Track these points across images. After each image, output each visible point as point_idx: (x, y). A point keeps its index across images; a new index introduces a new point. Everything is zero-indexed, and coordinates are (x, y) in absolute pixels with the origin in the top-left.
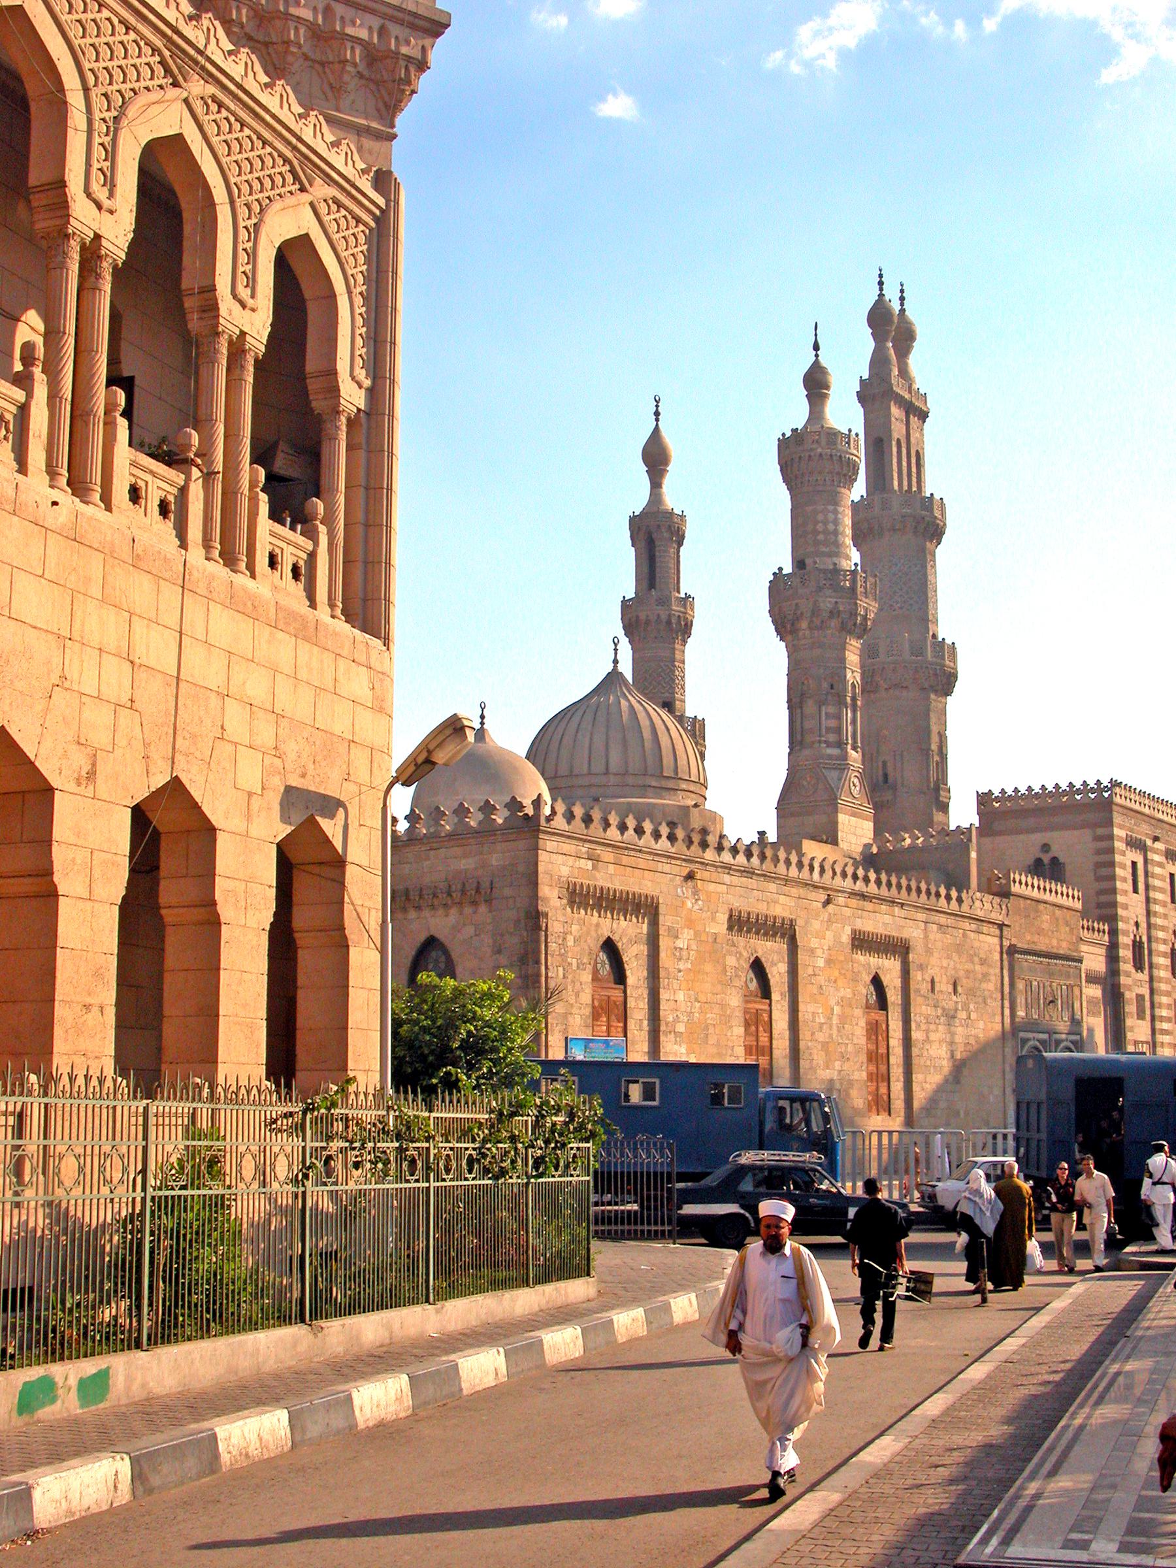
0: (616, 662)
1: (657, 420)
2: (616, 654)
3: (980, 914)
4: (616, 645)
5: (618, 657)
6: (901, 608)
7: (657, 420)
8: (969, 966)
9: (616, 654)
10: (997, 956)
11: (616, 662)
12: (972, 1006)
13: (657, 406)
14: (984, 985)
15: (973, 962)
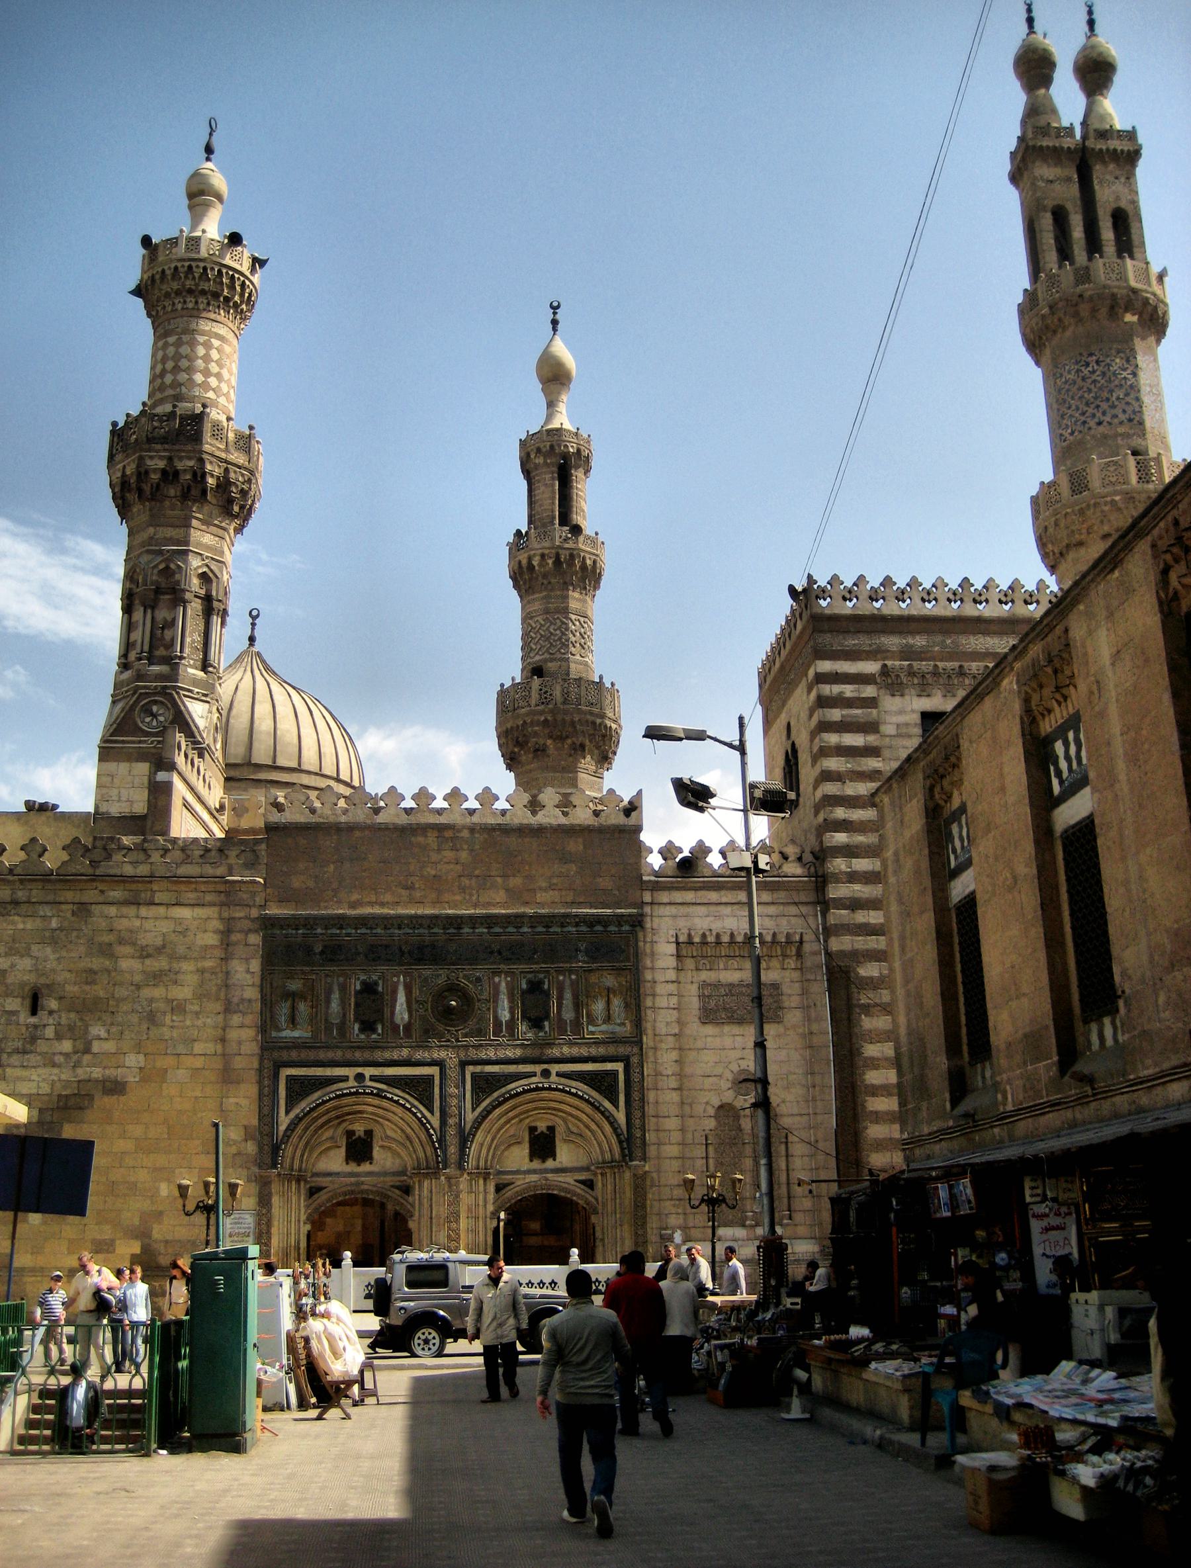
0: (252, 639)
1: (555, 330)
2: (253, 629)
3: (128, 870)
4: (254, 618)
5: (256, 634)
6: (1072, 433)
7: (555, 330)
8: (96, 963)
9: (253, 629)
10: (211, 939)
11: (252, 639)
12: (97, 1030)
13: (555, 313)
14: (158, 992)
15: (112, 956)
